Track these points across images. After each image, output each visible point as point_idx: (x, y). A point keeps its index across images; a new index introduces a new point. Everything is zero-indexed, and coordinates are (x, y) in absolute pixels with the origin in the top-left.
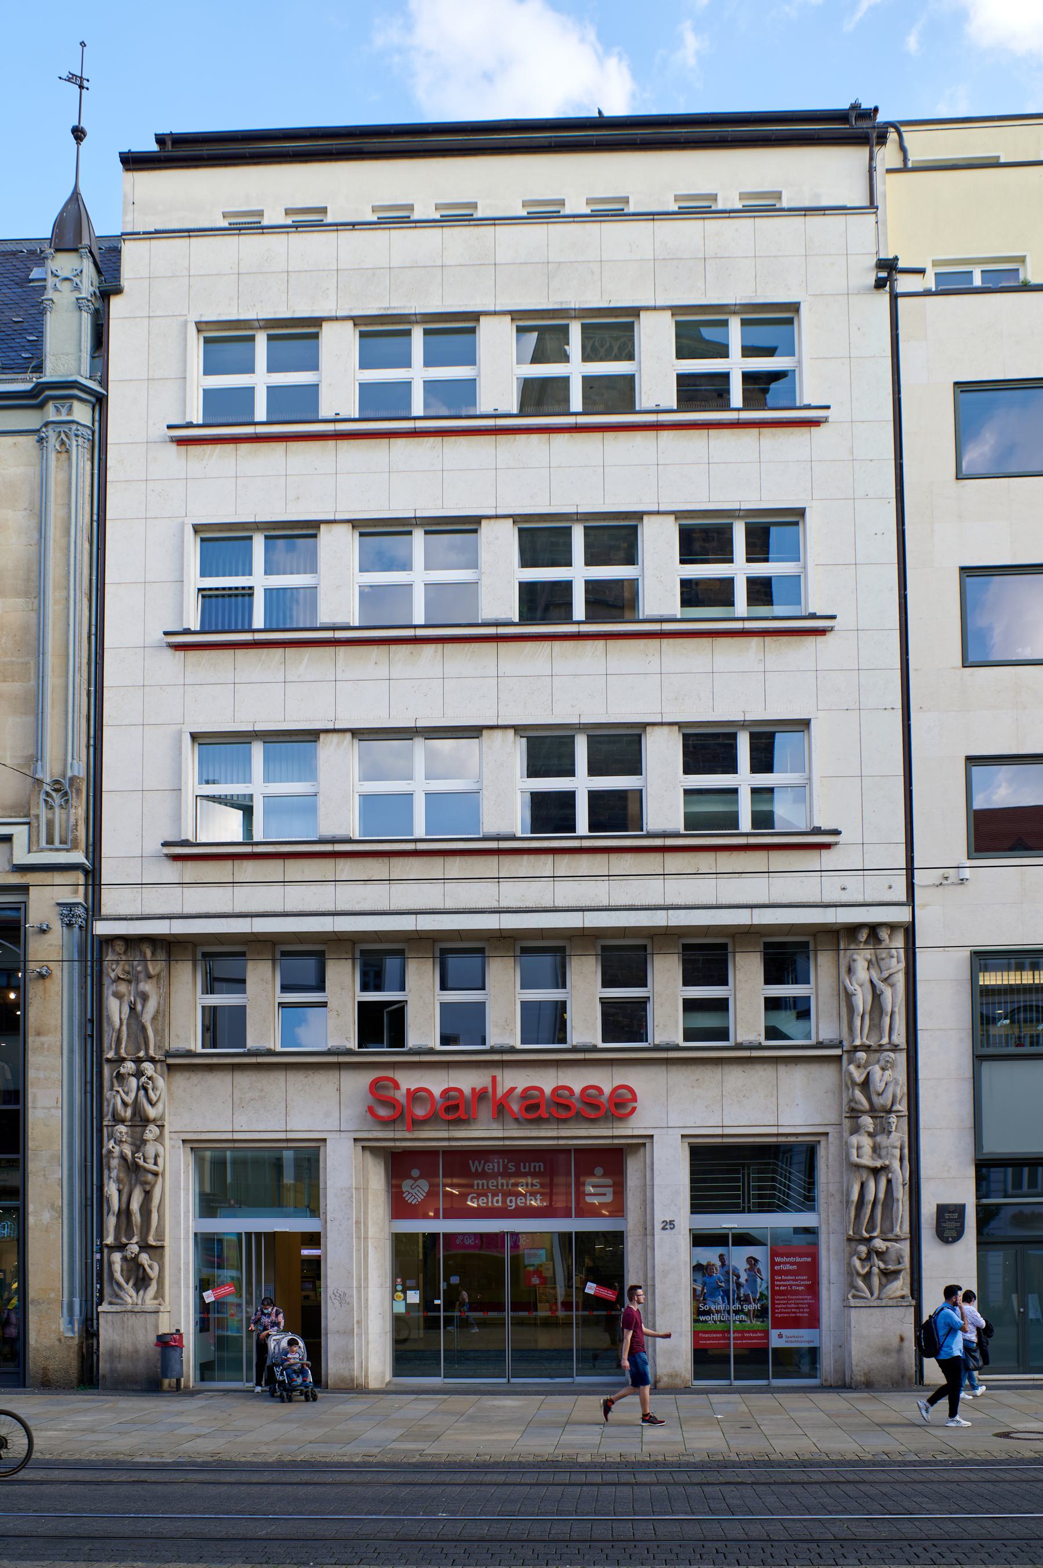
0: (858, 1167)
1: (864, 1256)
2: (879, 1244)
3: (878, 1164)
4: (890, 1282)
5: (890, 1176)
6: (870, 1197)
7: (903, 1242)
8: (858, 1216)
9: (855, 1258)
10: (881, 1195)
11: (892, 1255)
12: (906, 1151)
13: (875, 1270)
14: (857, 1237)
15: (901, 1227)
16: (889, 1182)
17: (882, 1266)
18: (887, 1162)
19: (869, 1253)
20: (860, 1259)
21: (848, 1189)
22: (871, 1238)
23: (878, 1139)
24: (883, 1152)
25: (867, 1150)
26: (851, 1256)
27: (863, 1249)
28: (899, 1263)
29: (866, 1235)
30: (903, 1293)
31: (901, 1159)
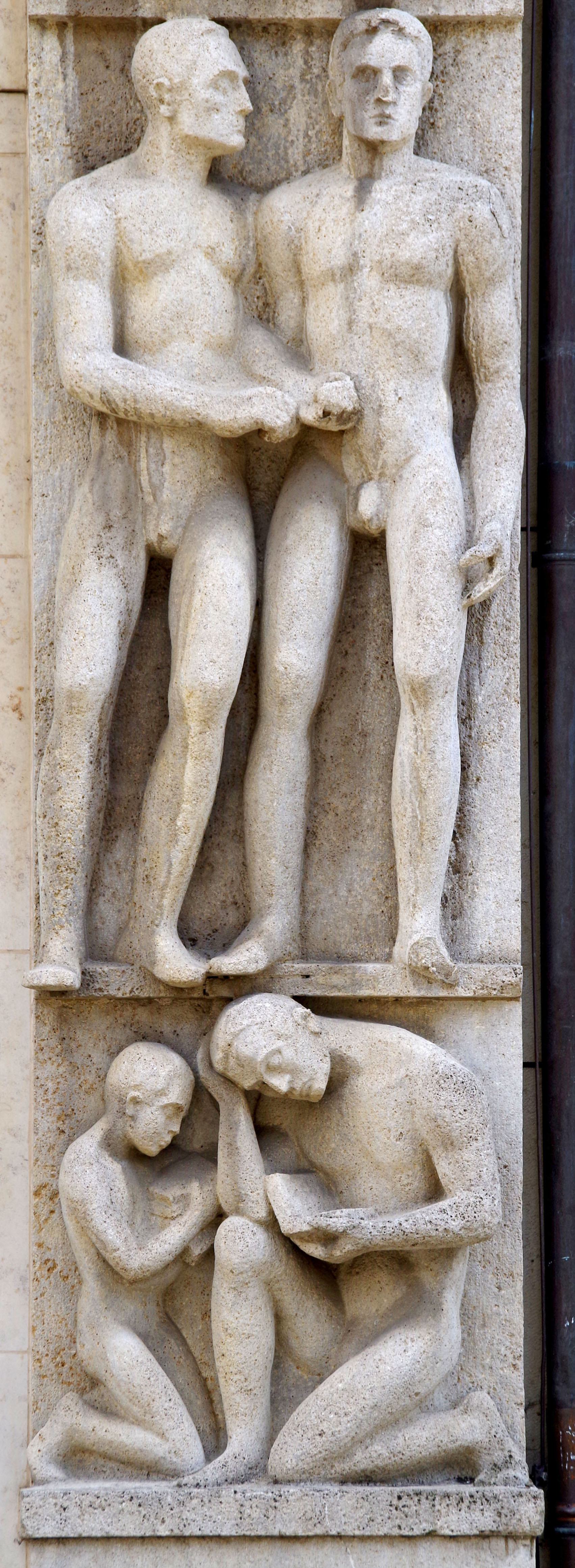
0: (118, 425)
1: (154, 1128)
2: (265, 1035)
3: (276, 403)
4: (353, 1336)
5: (368, 503)
6: (205, 663)
7: (470, 1028)
8: (117, 812)
9: (88, 1143)
10: (299, 655)
11: (377, 1128)
12: (502, 315)
13: (241, 1244)
14: (117, 981)
15: (453, 907)
16: (365, 551)
17: (295, 1206)
18: (339, 394)
19: (201, 1105)
20: (134, 1156)
21: (50, 603)
22: (218, 994)
23: (284, 205)
24: (324, 319)
25: (193, 294)
26: (70, 1127)
27: (152, 1076)
28: (435, 1191)
29: (178, 964)
30: (464, 1429)
31: (463, 375)
